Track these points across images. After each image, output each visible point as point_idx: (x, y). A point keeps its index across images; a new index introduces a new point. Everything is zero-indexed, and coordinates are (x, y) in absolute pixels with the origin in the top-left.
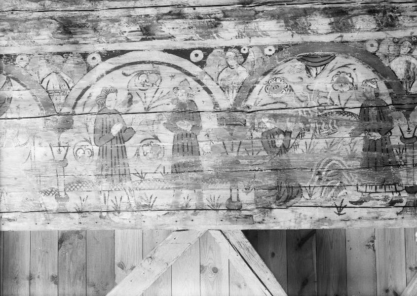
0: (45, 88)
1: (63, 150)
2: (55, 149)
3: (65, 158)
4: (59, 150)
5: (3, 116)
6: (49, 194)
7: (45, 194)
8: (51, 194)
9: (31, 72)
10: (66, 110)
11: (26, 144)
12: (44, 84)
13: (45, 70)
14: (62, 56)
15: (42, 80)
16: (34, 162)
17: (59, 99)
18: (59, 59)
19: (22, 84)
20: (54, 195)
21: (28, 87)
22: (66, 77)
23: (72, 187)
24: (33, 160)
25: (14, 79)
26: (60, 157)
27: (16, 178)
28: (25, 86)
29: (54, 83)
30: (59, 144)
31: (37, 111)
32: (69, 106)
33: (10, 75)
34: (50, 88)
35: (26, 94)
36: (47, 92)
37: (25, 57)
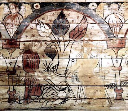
0: (108, 22)
1: (119, 60)
2: (114, 60)
3: (120, 65)
4: (117, 60)
5: (82, 39)
6: (111, 88)
7: (108, 88)
8: (112, 88)
9: (98, 13)
10: (120, 36)
11: (96, 56)
12: (107, 20)
13: (107, 11)
14: (118, 4)
15: (106, 18)
16: (101, 67)
17: (116, 29)
18: (116, 6)
19: (93, 20)
20: (114, 89)
21: (97, 22)
22: (120, 17)
23: (125, 83)
24: (100, 66)
25: (88, 16)
26: (117, 65)
27: (90, 77)
28: (95, 21)
29: (113, 19)
30: (117, 57)
31: (103, 36)
32: (122, 34)
33: (85, 14)
34: (111, 22)
35: (96, 27)
36: (109, 26)
37: (95, 5)
